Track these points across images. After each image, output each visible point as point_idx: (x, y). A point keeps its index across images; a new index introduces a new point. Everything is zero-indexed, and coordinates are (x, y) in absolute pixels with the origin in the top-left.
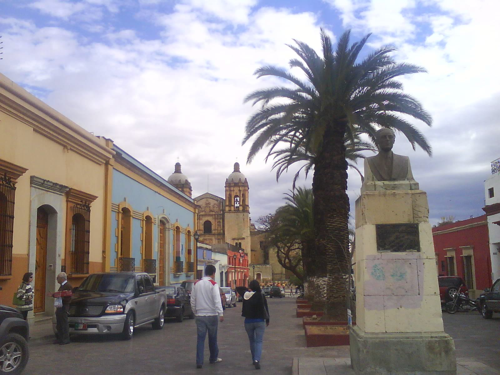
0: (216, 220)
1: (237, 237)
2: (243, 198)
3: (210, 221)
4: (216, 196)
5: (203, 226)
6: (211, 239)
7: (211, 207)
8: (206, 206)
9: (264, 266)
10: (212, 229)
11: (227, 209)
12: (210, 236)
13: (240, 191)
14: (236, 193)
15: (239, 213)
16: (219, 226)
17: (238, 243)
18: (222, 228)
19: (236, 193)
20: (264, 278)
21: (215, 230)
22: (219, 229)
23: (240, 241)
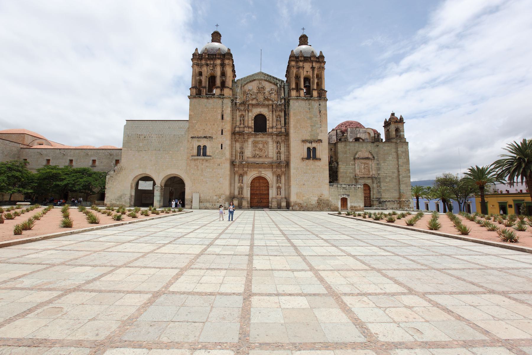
0: (274, 113)
1: (309, 138)
2: (318, 79)
3: (265, 114)
4: (274, 78)
5: (253, 122)
6: (267, 143)
7: (267, 93)
8: (258, 91)
9: (353, 186)
10: (267, 127)
11: (294, 93)
12: (264, 136)
13: (313, 68)
14: (307, 72)
15: (313, 102)
16: (279, 123)
17: (311, 149)
18: (283, 125)
19: (307, 72)
20: (353, 204)
21: (272, 127)
22: (279, 126)
23: (314, 145)
